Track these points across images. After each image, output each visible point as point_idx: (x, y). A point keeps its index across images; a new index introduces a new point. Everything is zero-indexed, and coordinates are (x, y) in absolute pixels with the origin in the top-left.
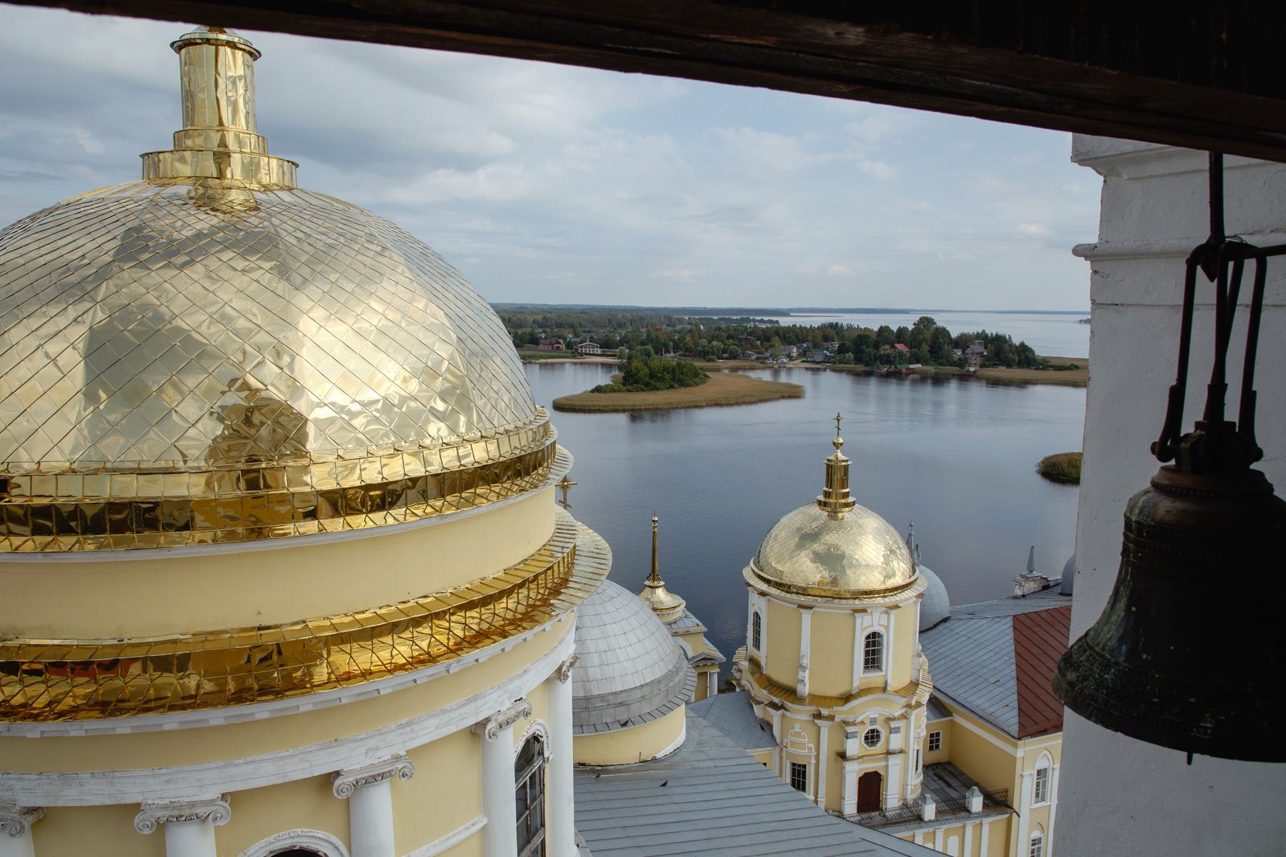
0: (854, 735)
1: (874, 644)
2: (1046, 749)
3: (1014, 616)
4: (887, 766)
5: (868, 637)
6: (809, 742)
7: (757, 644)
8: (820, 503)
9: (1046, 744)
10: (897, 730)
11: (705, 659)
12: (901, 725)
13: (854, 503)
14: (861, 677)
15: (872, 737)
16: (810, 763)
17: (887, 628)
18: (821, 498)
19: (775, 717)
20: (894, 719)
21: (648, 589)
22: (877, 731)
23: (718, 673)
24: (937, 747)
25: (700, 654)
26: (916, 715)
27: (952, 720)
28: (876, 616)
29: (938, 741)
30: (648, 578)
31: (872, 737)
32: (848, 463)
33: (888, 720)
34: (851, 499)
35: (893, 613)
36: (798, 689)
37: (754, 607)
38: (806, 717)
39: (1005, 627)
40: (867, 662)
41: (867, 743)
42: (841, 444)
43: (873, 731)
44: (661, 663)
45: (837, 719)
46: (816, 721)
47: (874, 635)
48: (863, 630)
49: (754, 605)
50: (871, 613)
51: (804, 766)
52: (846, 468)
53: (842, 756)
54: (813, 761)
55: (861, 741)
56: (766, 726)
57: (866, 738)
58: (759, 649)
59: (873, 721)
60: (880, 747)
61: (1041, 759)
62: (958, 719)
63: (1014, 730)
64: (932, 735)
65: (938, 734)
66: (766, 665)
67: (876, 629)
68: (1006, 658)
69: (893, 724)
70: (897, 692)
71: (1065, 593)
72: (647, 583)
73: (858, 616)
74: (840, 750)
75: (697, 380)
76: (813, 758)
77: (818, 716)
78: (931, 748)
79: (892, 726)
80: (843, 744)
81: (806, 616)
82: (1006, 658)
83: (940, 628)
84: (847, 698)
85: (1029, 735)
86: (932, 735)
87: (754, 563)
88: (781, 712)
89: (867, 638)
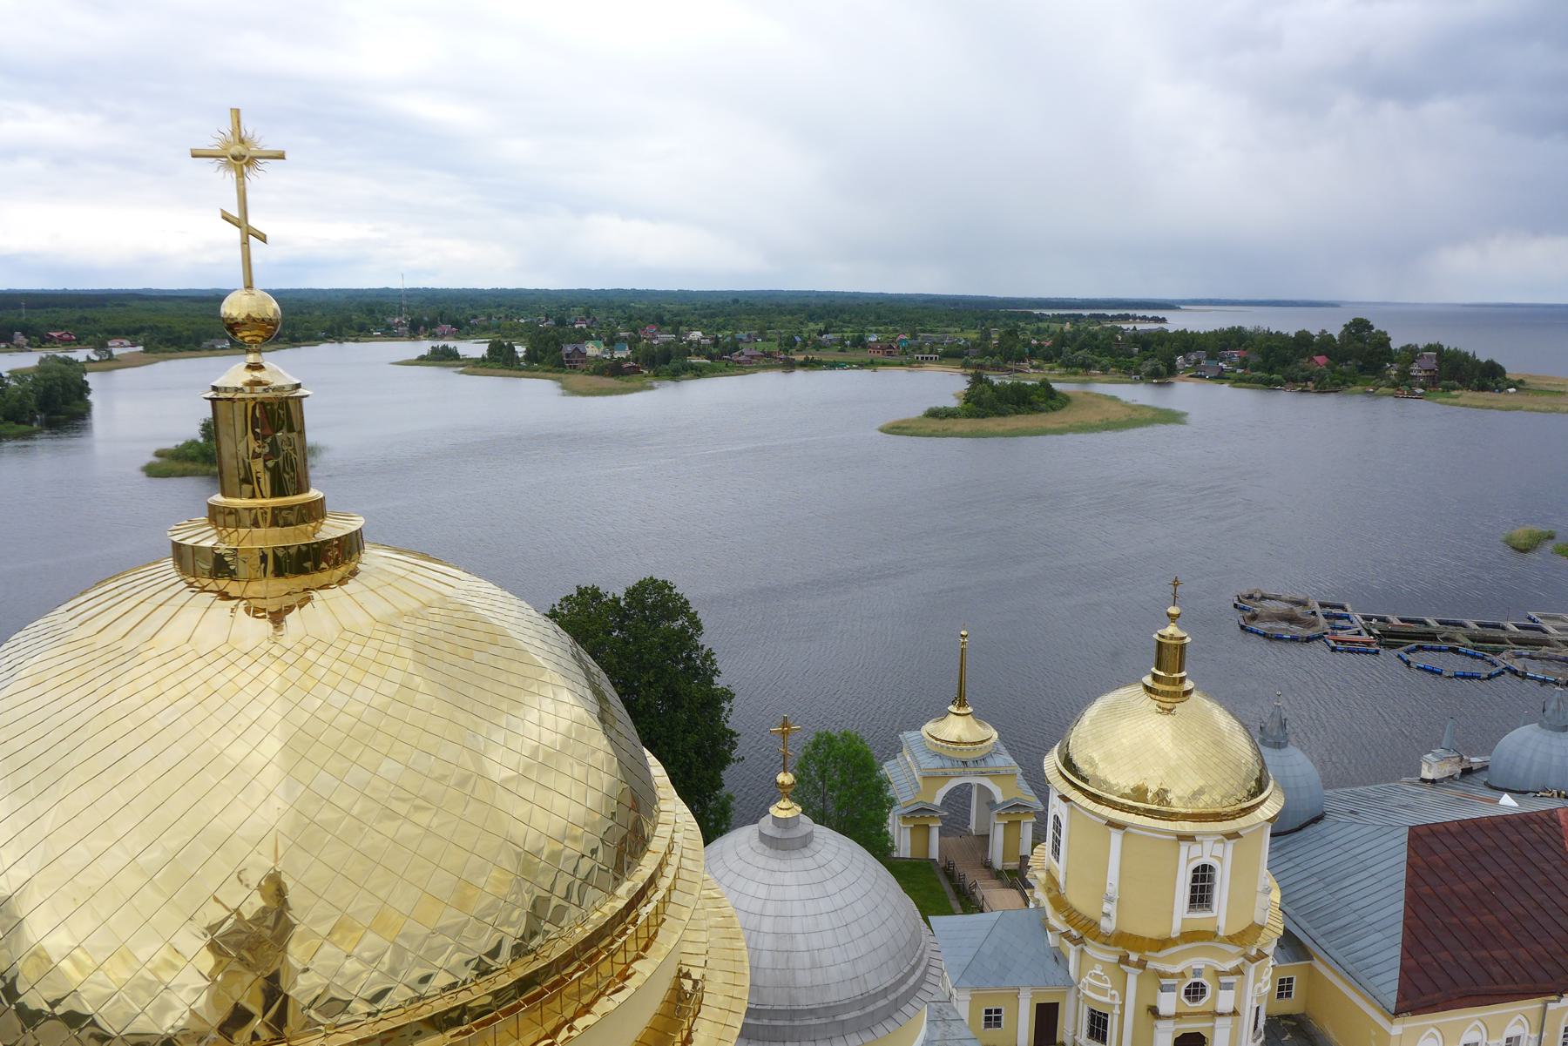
0: (1171, 988)
1: (1203, 879)
2: (1434, 1026)
3: (1411, 828)
4: (1213, 1027)
5: (1196, 870)
6: (1111, 989)
7: (1056, 851)
8: (1148, 689)
9: (1437, 1021)
10: (1228, 986)
11: (1017, 805)
12: (1235, 981)
13: (1187, 693)
14: (1181, 915)
15: (1195, 992)
16: (1113, 1014)
17: (1221, 860)
18: (1148, 680)
19: (1072, 952)
20: (1224, 973)
21: (952, 716)
22: (1202, 985)
23: (1034, 824)
24: (1289, 995)
25: (1012, 800)
26: (1256, 967)
27: (1310, 964)
28: (1208, 845)
29: (1289, 988)
30: (953, 703)
31: (1195, 992)
32: (1188, 640)
33: (1218, 973)
34: (1188, 685)
35: (1230, 844)
36: (1102, 924)
37: (1054, 810)
38: (1114, 958)
39: (1398, 842)
40: (1193, 900)
41: (1189, 998)
42: (1178, 616)
43: (1196, 984)
44: (890, 962)
45: (1151, 965)
46: (1122, 966)
47: (1204, 866)
48: (1189, 861)
49: (1054, 806)
50: (1201, 842)
51: (1106, 1015)
52: (1182, 648)
53: (1154, 1011)
54: (1117, 1011)
55: (1178, 997)
56: (1059, 958)
57: (1187, 992)
58: (1058, 861)
59: (1197, 973)
60: (1202, 1005)
61: (1426, 1038)
62: (1317, 964)
63: (1391, 1000)
64: (1282, 981)
65: (1290, 980)
66: (1065, 882)
67: (1207, 860)
68: (1392, 890)
69: (1224, 980)
70: (1231, 939)
71: (1493, 785)
72: (952, 708)
73: (1184, 846)
74: (1152, 1004)
75: (1051, 402)
76: (1117, 1007)
77: (1124, 960)
78: (1280, 996)
79: (1221, 981)
80: (1155, 997)
81: (1116, 837)
82: (1392, 890)
83: (1309, 830)
84: (1163, 943)
85: (1410, 1011)
86: (1282, 981)
87: (1058, 753)
88: (1079, 946)
89: (1194, 871)
